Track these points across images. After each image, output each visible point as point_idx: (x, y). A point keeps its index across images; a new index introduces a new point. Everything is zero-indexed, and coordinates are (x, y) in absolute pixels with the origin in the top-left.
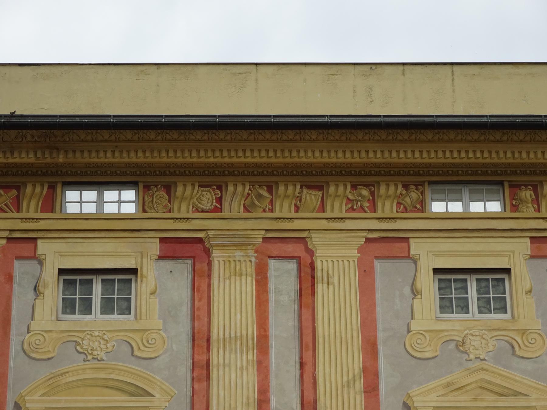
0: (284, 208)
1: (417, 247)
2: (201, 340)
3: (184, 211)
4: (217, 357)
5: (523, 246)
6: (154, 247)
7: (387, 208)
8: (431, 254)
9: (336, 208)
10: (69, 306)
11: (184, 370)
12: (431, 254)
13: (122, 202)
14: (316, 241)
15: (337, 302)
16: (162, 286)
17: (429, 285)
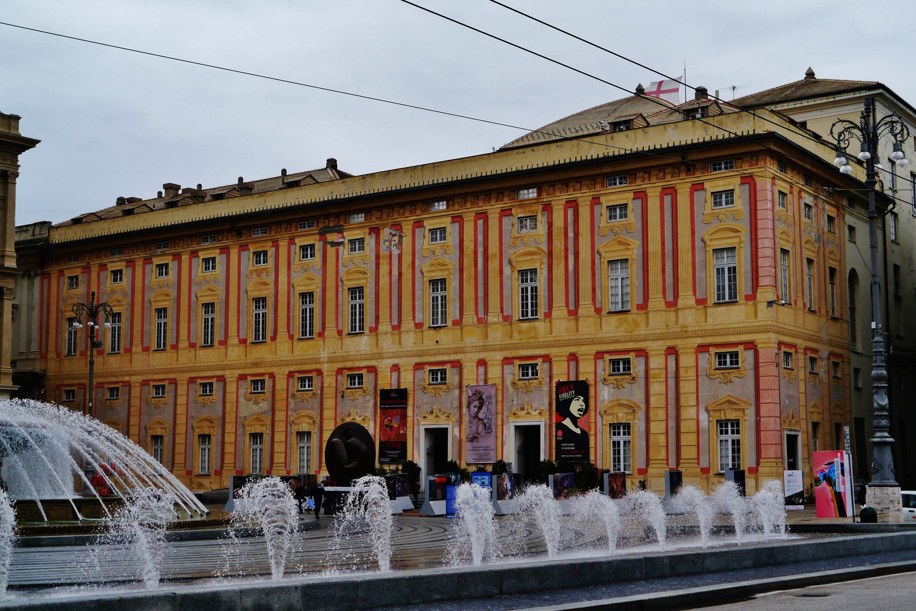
0: (395, 216)
1: (425, 223)
2: (378, 257)
3: (374, 219)
4: (381, 261)
5: (449, 219)
6: (367, 230)
7: (418, 212)
8: (429, 224)
9: (407, 214)
10: (352, 250)
11: (374, 266)
12: (429, 224)
13: (360, 218)
14: (403, 224)
15: (407, 241)
16: (370, 242)
17: (428, 235)
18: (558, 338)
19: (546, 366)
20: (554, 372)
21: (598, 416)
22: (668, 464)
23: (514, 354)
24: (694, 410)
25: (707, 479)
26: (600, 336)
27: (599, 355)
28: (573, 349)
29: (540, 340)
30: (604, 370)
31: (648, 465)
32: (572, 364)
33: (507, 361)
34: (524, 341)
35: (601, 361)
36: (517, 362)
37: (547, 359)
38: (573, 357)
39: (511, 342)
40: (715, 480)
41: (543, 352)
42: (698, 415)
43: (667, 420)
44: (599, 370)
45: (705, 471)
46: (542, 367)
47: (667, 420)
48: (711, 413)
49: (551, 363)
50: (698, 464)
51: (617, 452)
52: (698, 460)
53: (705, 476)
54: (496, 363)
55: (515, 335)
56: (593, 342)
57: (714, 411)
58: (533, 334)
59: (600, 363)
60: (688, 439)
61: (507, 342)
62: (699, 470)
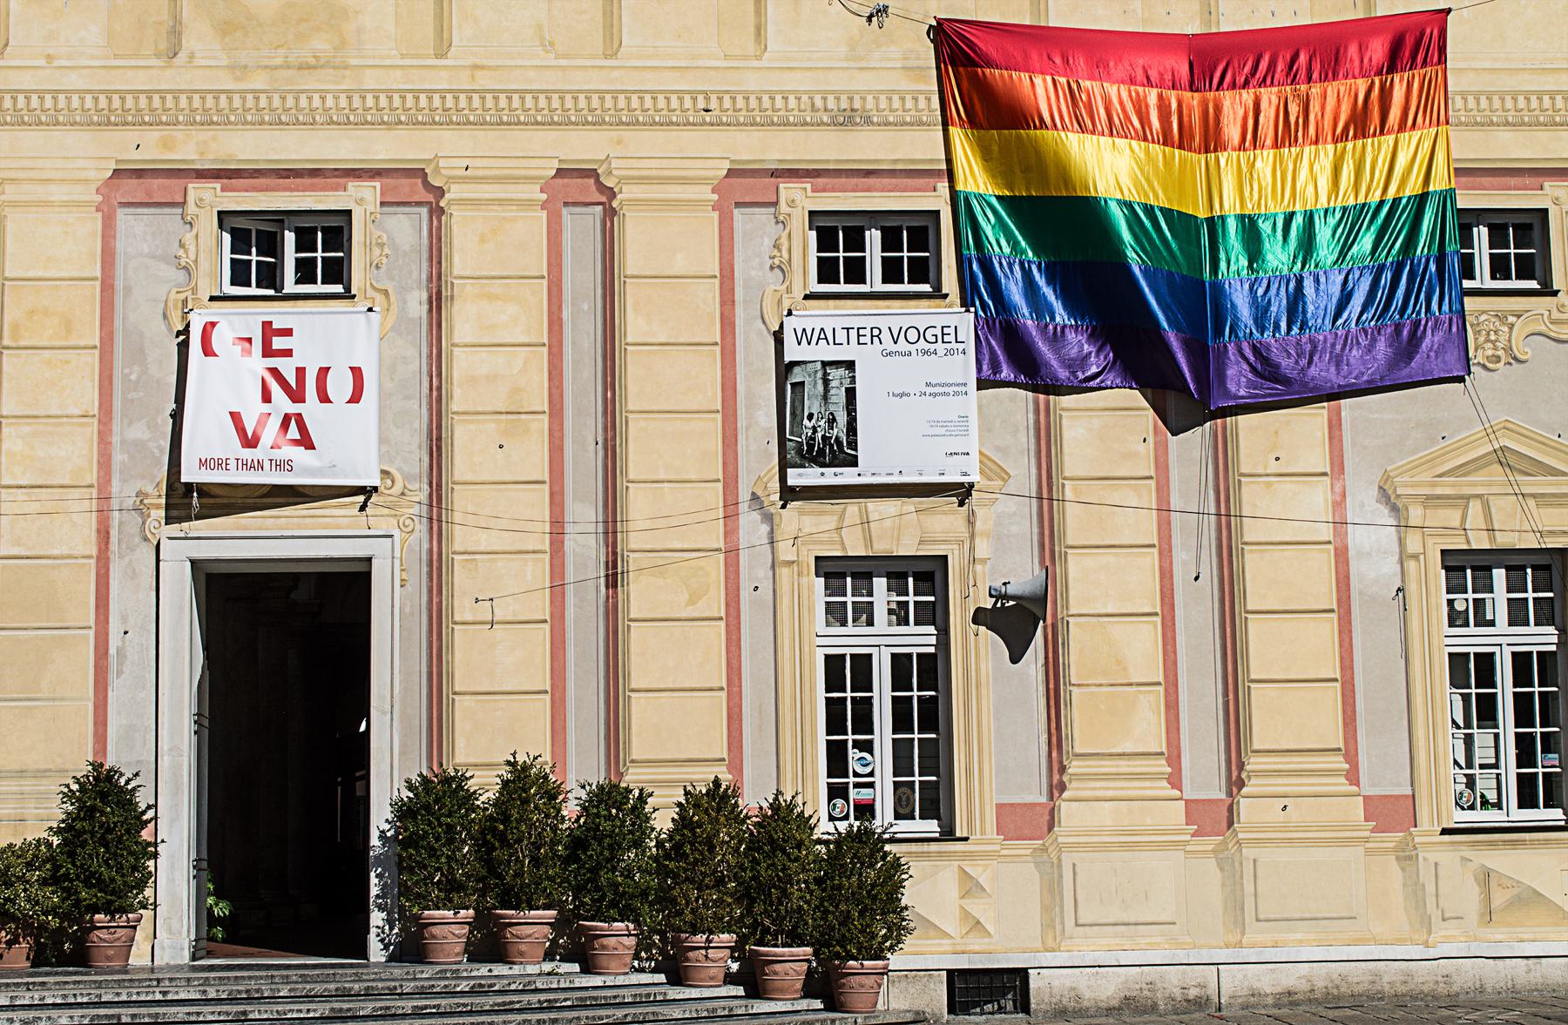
18: (484, 81)
19: (407, 228)
20: (462, 259)
21: (751, 526)
22: (1175, 781)
23: (189, 149)
24: (1317, 497)
25: (1406, 856)
26: (753, 82)
27: (748, 186)
28: (582, 147)
29: (370, 81)
30: (782, 269)
31: (1057, 788)
32: (581, 227)
33: (143, 185)
34: (259, 82)
35: (763, 215)
36: (209, 199)
37: (418, 189)
38: (585, 188)
39: (169, 79)
40: (1451, 859)
41: (384, 148)
42: (1340, 524)
43: (1165, 550)
44: (751, 267)
45: (1391, 814)
46: (383, 239)
47: (1165, 550)
48: (1416, 515)
49: (437, 212)
50: (1353, 777)
51: (847, 719)
52: (1350, 752)
53: (1393, 838)
54: (58, 193)
55: (199, 39)
56: (707, 114)
57: (1431, 501)
58: (321, 44)
59: (752, 226)
60: (1285, 648)
61: (140, 81)
62: (1358, 808)
